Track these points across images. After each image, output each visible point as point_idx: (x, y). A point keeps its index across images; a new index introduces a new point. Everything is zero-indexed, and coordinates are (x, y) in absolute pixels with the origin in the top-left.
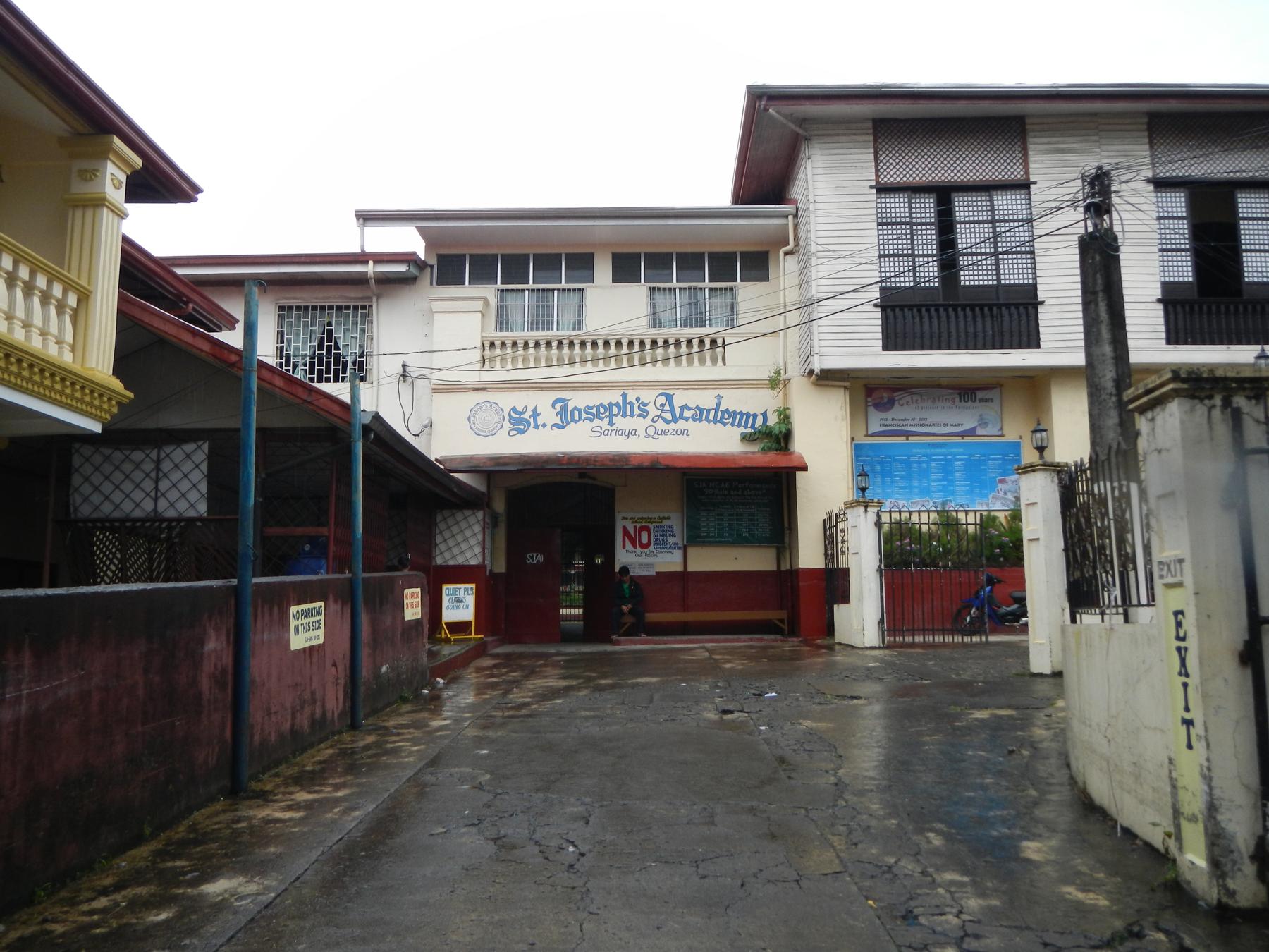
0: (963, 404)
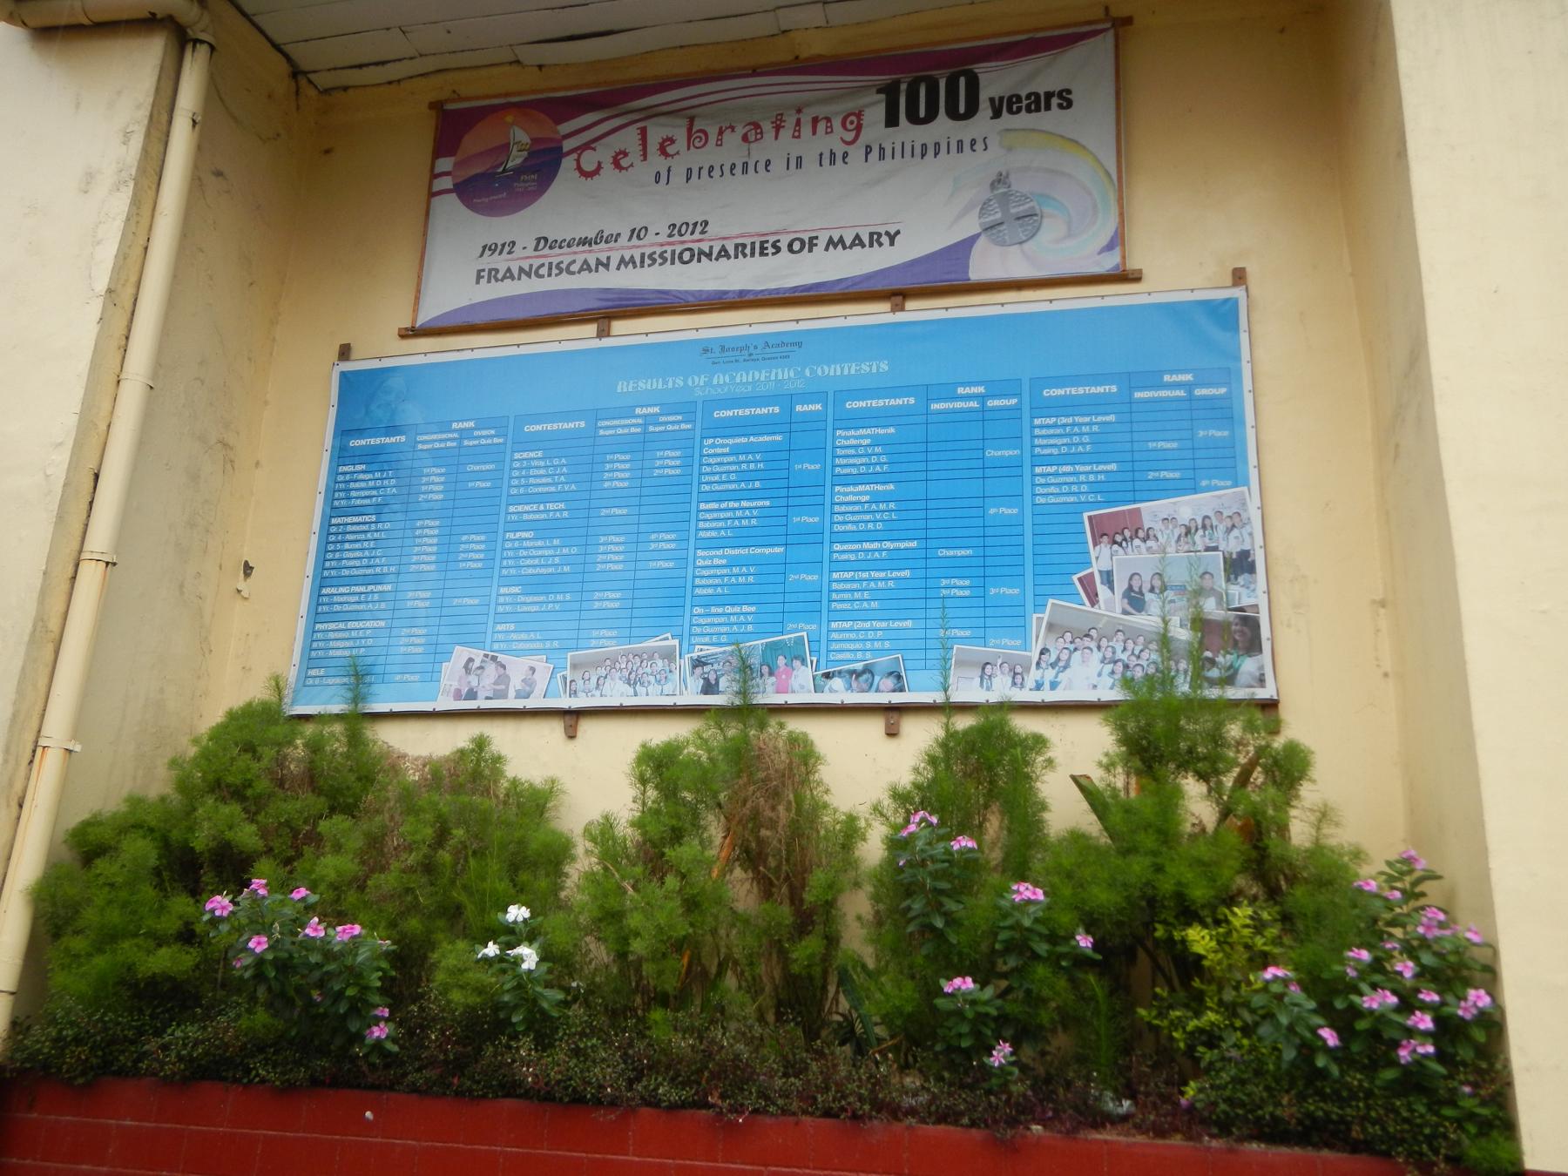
0: (907, 132)
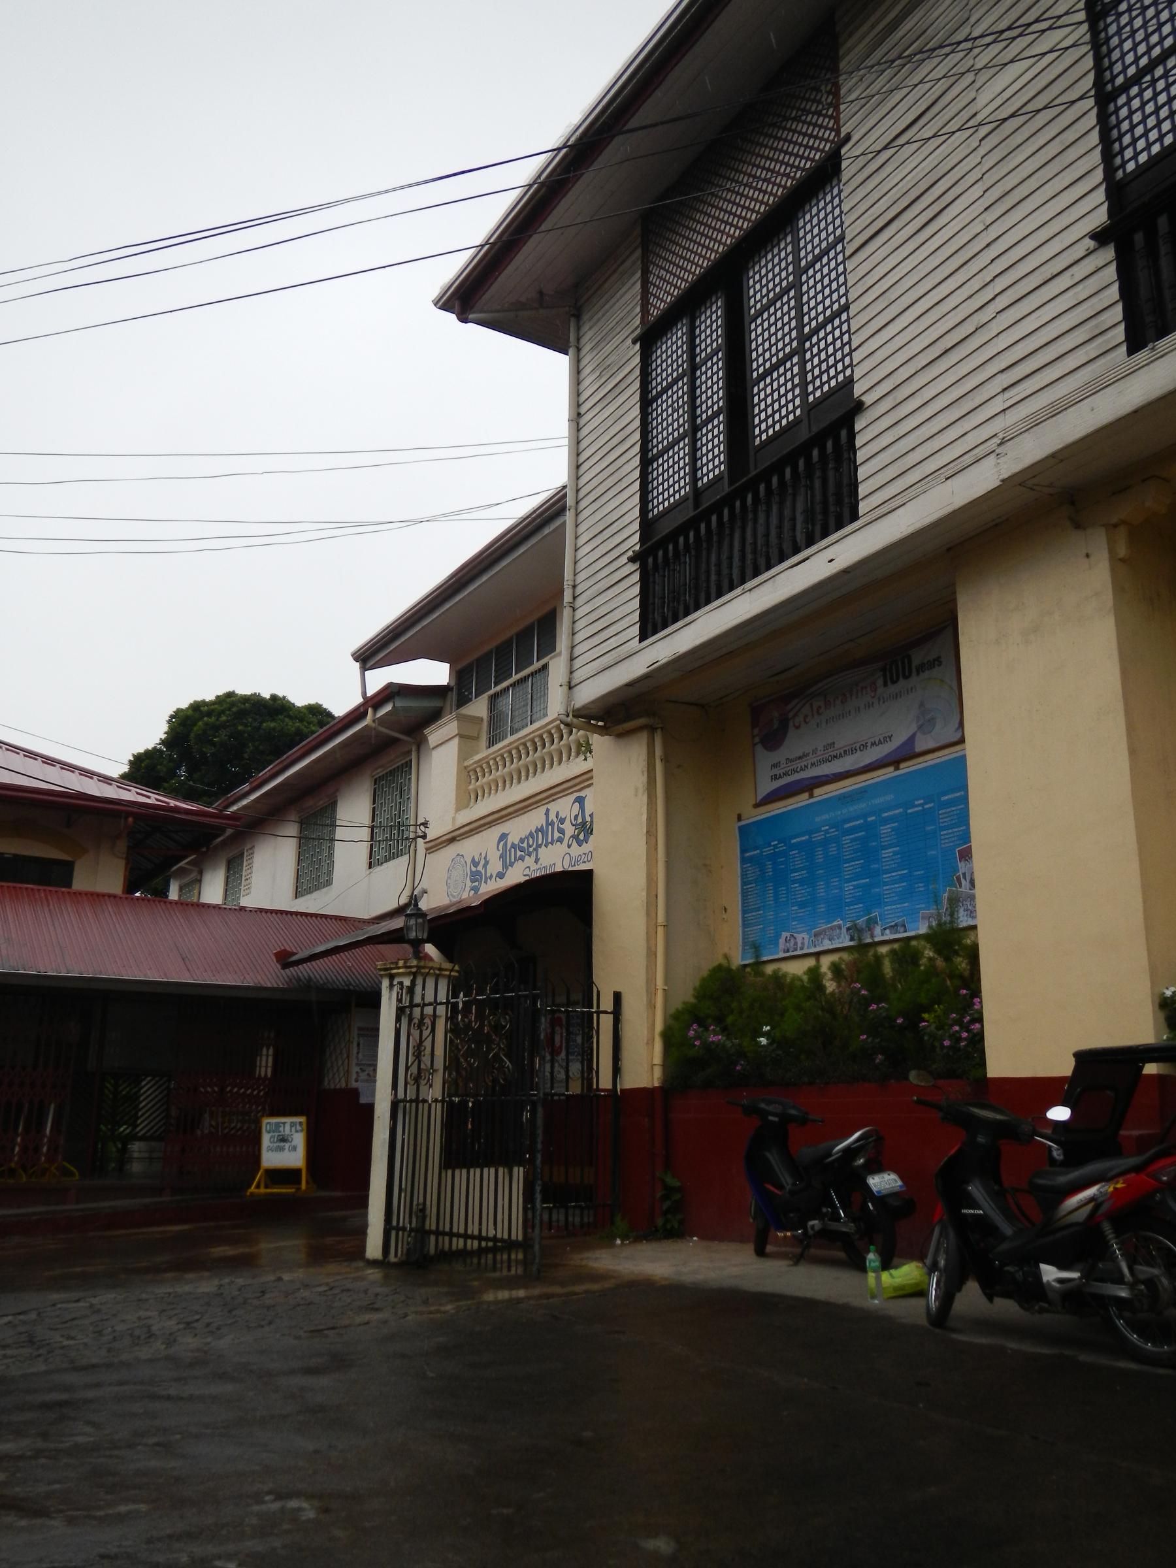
0: (893, 689)
